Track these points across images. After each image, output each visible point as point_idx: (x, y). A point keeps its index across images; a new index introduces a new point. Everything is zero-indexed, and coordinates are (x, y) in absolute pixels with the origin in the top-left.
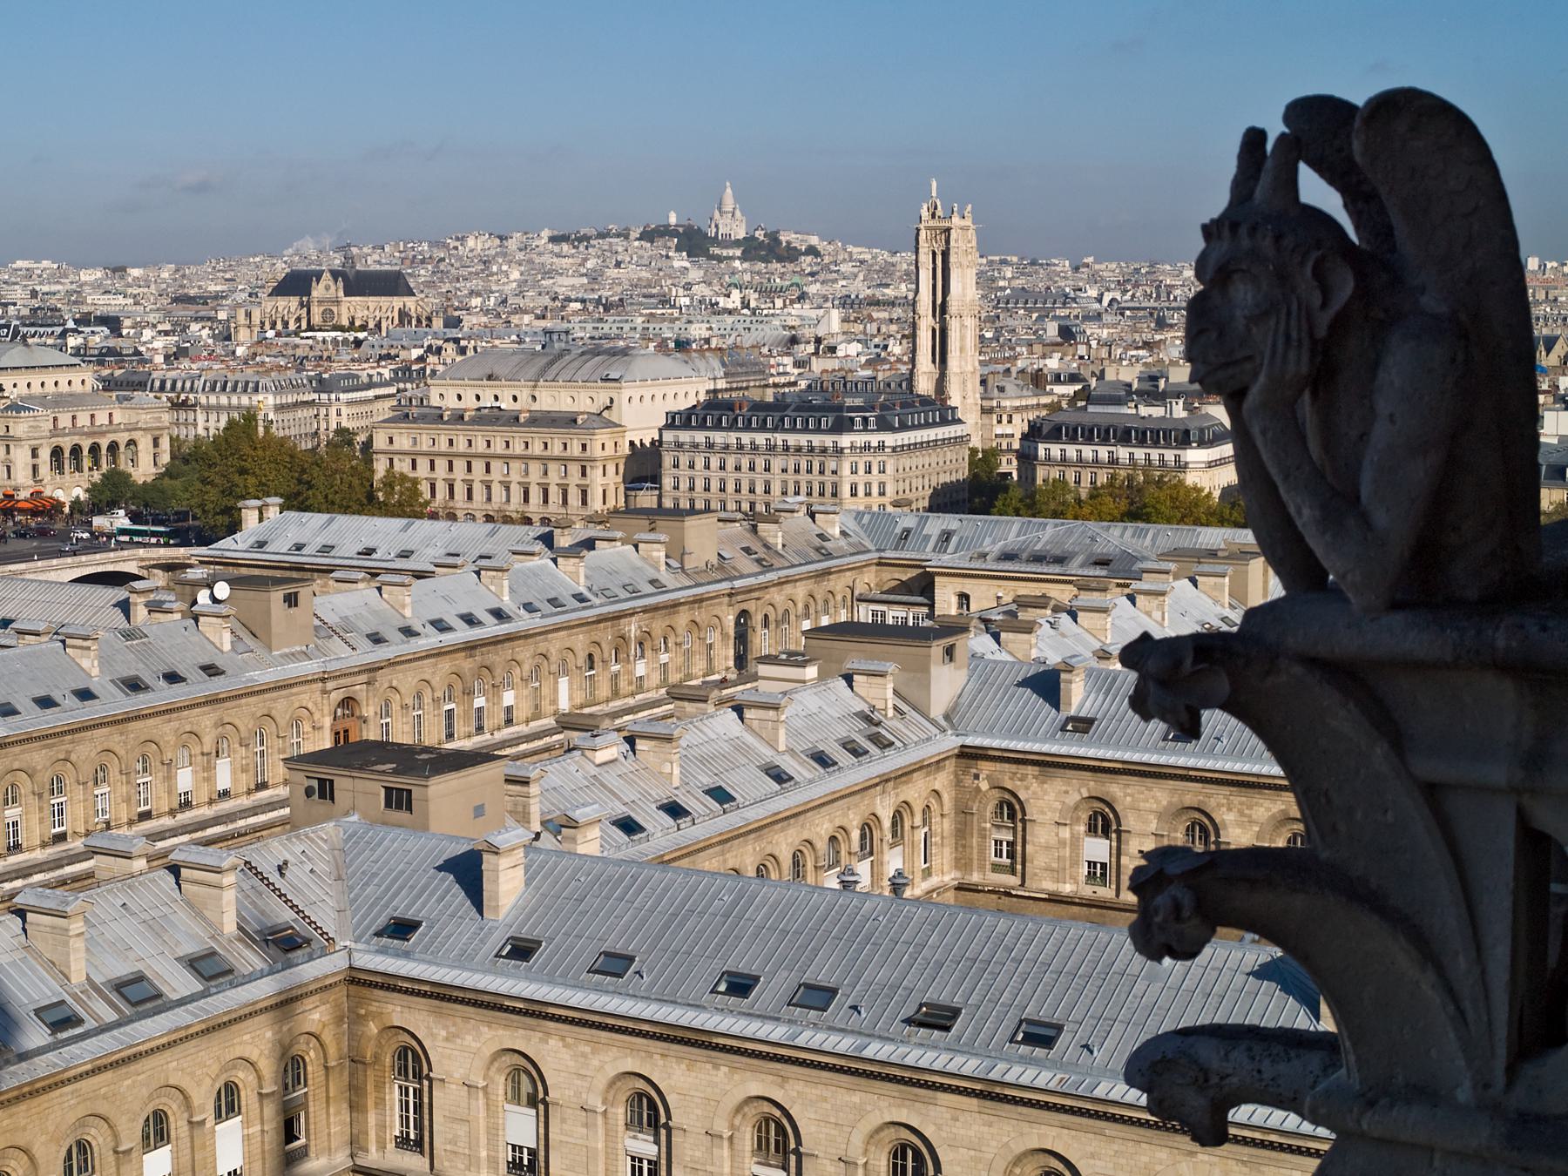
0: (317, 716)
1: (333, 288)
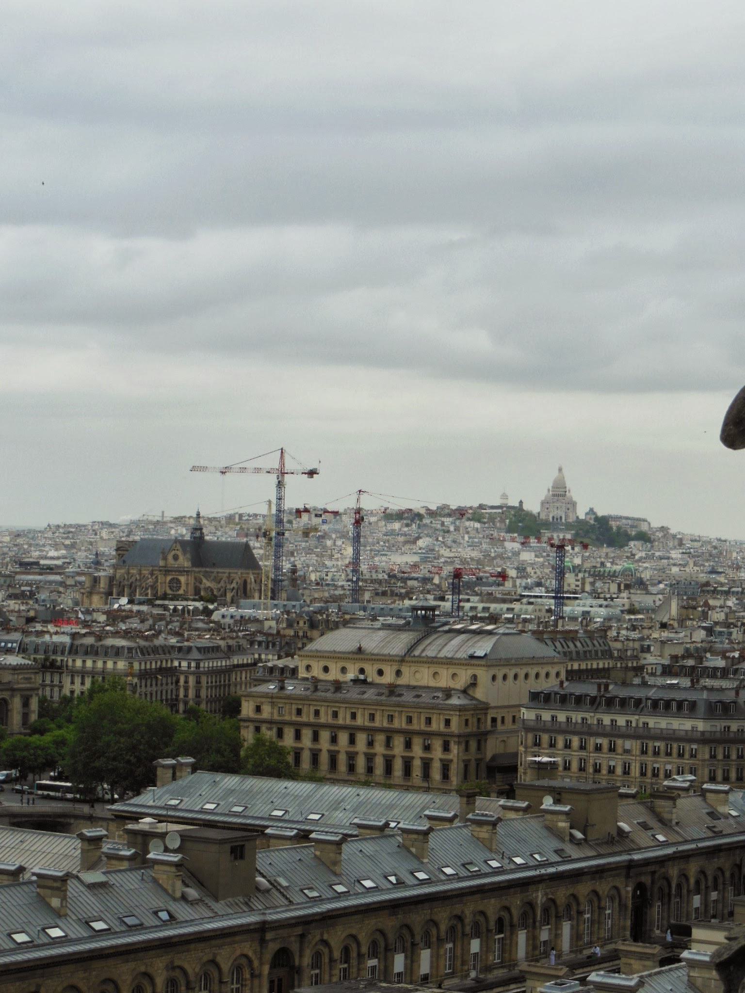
0: (256, 963)
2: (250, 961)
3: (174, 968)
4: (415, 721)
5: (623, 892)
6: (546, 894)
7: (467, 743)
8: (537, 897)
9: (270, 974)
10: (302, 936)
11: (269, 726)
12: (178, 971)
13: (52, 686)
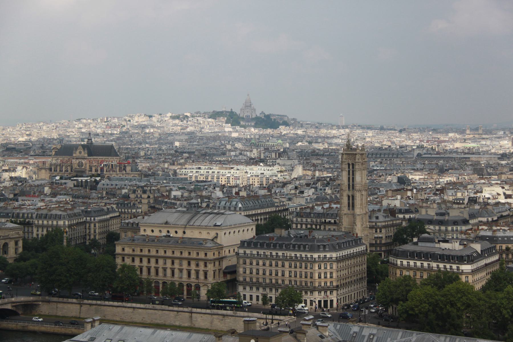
1: (83, 152)
4: (191, 254)
7: (214, 263)
11: (128, 257)
13: (28, 232)
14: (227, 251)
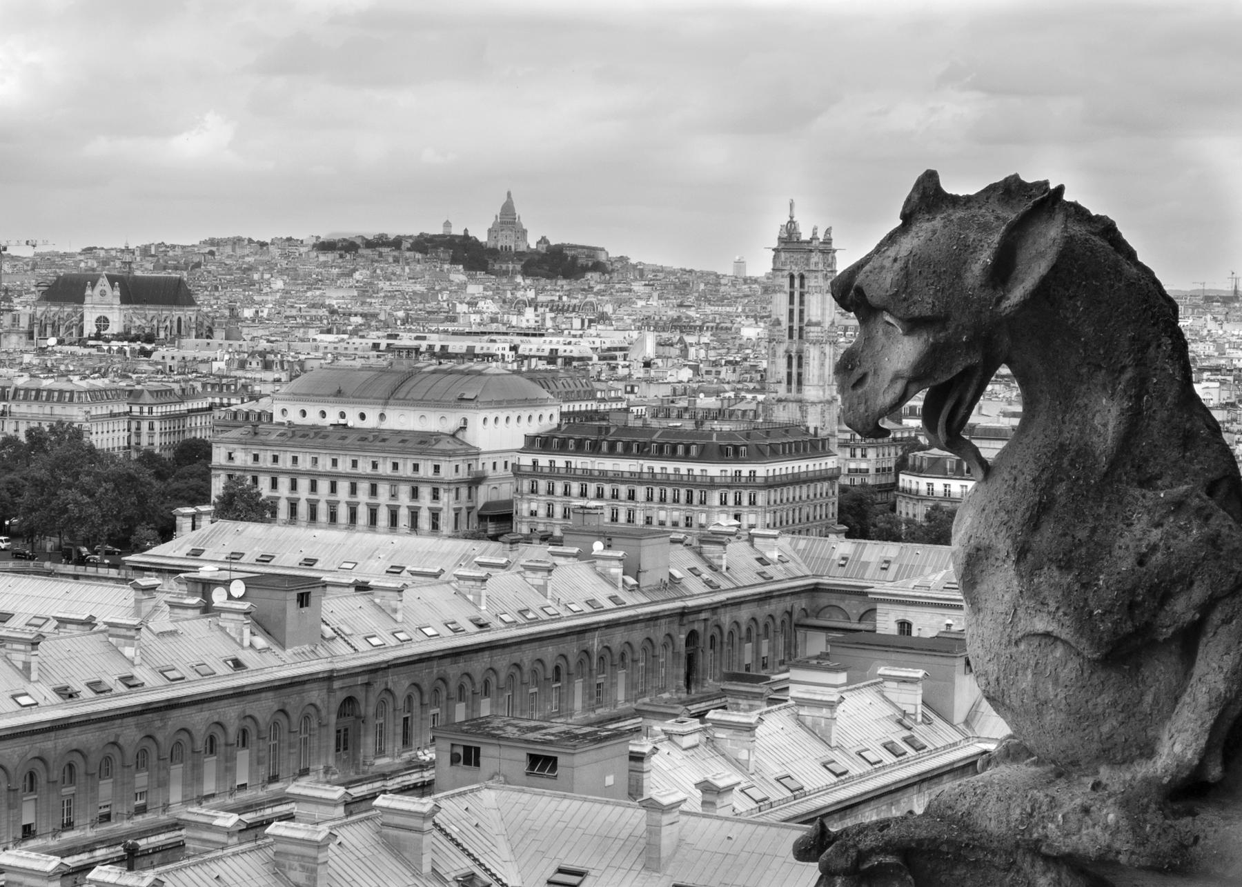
0: (324, 713)
2: (318, 710)
3: (245, 717)
4: (400, 467)
5: (677, 641)
6: (602, 642)
8: (593, 645)
9: (337, 723)
10: (368, 684)
12: (249, 720)
14: (489, 467)
